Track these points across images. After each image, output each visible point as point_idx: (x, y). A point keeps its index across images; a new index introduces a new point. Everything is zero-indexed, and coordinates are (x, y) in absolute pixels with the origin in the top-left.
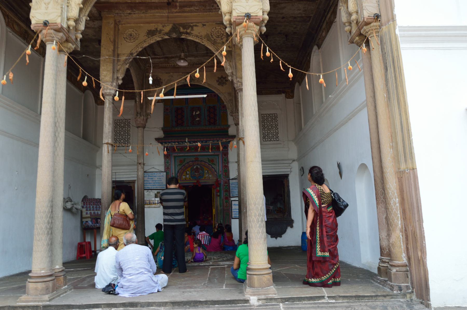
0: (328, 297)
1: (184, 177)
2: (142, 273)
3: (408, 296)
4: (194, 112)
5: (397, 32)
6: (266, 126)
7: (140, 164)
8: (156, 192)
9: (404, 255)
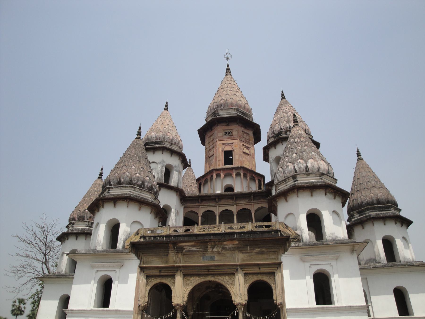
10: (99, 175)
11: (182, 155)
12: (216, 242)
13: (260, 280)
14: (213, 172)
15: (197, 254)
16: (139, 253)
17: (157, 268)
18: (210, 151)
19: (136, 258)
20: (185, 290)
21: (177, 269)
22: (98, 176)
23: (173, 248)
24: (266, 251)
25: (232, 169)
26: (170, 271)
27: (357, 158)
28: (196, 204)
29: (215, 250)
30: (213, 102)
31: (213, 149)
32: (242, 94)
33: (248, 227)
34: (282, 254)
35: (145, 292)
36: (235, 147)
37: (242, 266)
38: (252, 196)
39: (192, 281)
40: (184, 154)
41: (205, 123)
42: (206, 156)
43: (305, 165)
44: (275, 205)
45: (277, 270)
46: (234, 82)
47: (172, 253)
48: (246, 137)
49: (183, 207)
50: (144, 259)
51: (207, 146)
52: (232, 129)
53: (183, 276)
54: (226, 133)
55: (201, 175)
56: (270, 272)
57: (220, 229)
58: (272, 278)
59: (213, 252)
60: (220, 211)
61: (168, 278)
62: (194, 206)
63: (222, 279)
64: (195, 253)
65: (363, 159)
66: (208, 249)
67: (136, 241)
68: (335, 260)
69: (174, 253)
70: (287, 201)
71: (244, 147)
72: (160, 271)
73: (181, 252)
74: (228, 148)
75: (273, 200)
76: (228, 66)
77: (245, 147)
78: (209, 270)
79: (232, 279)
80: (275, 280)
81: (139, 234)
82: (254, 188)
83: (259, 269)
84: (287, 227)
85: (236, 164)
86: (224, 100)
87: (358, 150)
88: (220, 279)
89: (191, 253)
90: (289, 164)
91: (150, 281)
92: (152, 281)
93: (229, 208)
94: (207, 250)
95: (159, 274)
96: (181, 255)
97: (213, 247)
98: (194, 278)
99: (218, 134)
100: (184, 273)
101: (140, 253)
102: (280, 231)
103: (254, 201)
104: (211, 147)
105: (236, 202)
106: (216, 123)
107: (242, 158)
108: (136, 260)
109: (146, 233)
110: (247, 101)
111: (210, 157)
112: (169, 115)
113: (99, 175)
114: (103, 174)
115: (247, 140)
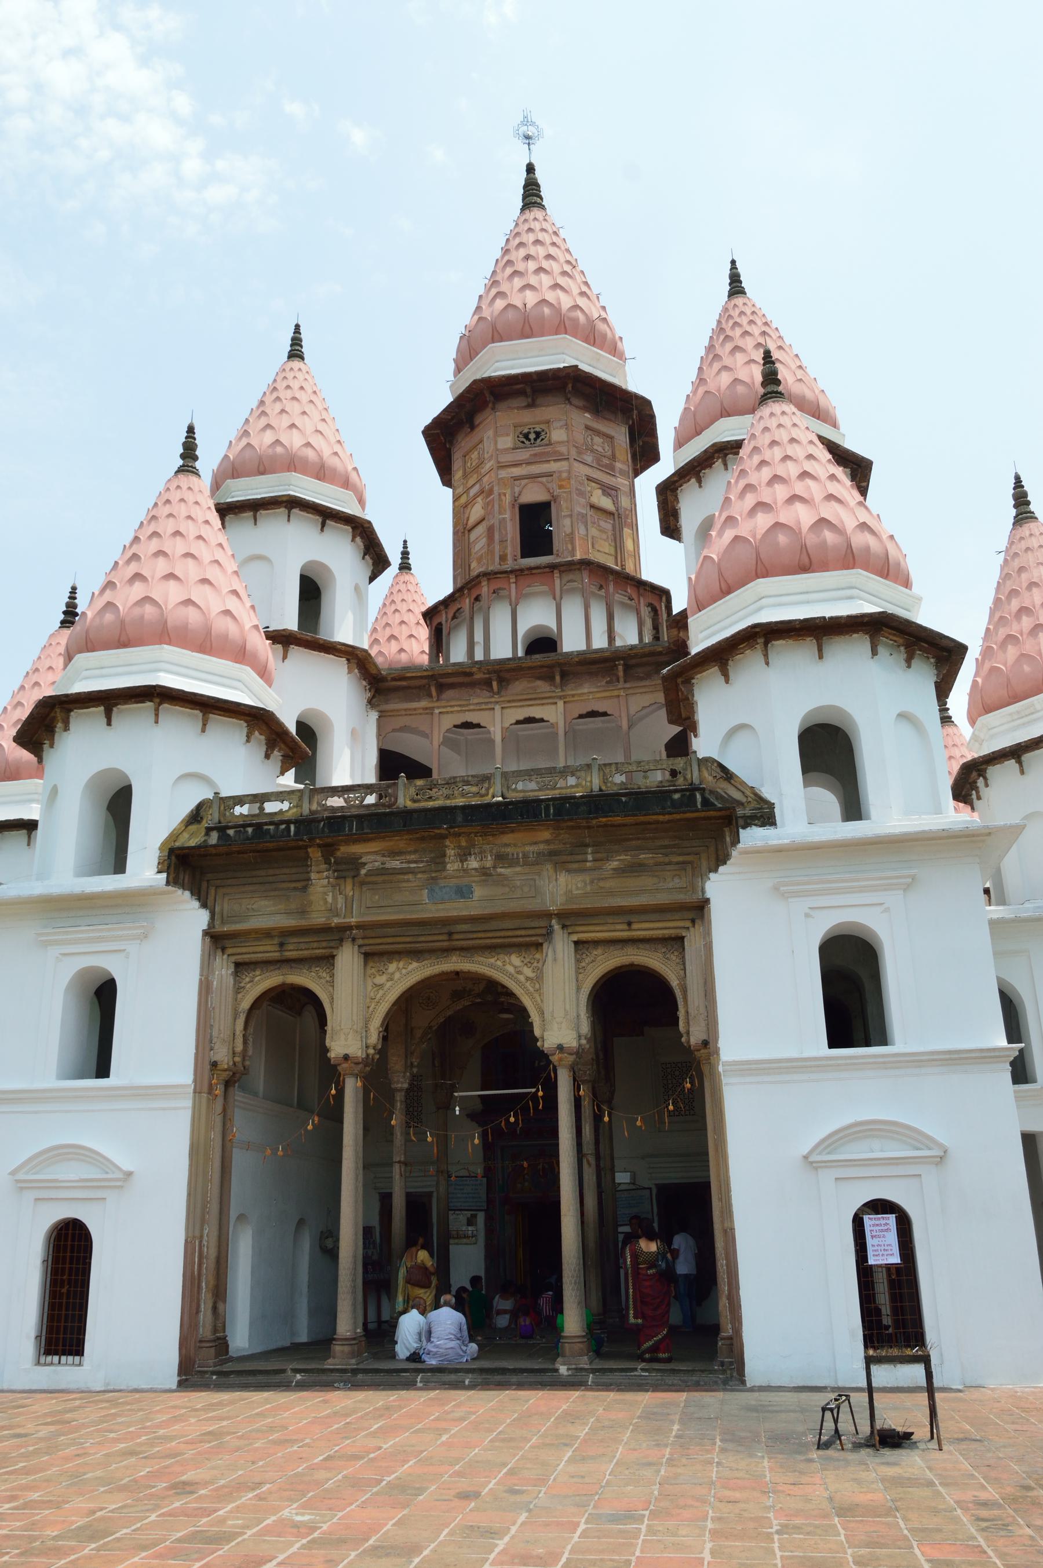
0: (641, 1369)
1: (519, 1186)
2: (450, 1340)
3: (729, 1372)
4: (537, 1062)
5: (721, 1069)
6: (670, 1086)
7: (442, 1172)
8: (469, 1214)
9: (730, 1326)
10: (64, 613)
11: (362, 526)
12: (473, 835)
13: (632, 965)
14: (480, 582)
15: (408, 881)
16: (204, 885)
17: (267, 934)
18: (469, 506)
19: (196, 904)
20: (371, 1009)
21: (338, 934)
22: (62, 617)
23: (326, 864)
24: (652, 861)
25: (547, 570)
26: (315, 945)
27: (1014, 512)
28: (419, 699)
29: (473, 863)
30: (476, 317)
31: (479, 499)
32: (586, 283)
33: (589, 779)
34: (710, 872)
35: (235, 1018)
36: (561, 487)
37: (569, 918)
38: (621, 668)
39: (393, 974)
40: (369, 522)
41: (449, 399)
42: (455, 525)
44: (688, 699)
45: (692, 929)
46: (555, 233)
47: (320, 881)
48: (600, 449)
49: (374, 716)
50: (225, 906)
51: (460, 490)
52: (548, 422)
53: (362, 960)
54: (526, 436)
55: (441, 597)
56: (667, 936)
57: (488, 789)
58: (674, 958)
59: (465, 871)
60: (507, 725)
61: (310, 967)
62: (415, 709)
63: (499, 963)
64: (402, 877)
65: (1037, 515)
66: (447, 860)
67: (193, 845)
68: (902, 892)
69: (329, 881)
71: (594, 484)
72: (281, 945)
73: (354, 877)
74: (533, 495)
75: (679, 680)
76: (530, 169)
77: (599, 486)
78: (450, 934)
79: (535, 964)
80: (684, 964)
81: (202, 818)
82: (629, 635)
83: (625, 927)
84: (727, 774)
85: (563, 551)
86: (515, 307)
87: (1018, 482)
88: (491, 966)
89: (386, 878)
91: (248, 979)
92: (257, 979)
93: (536, 712)
94: (444, 864)
95: (277, 954)
96: (354, 885)
97: (465, 855)
98: (401, 965)
99: (496, 443)
100: (363, 950)
101: (208, 887)
102: (704, 789)
103: (628, 685)
104: (473, 492)
105: (563, 690)
106: (488, 399)
107: (587, 530)
108: (194, 909)
109: (228, 814)
110: (604, 308)
111: (469, 531)
112: (307, 376)
113: (64, 613)
114: (77, 610)
115: (606, 461)
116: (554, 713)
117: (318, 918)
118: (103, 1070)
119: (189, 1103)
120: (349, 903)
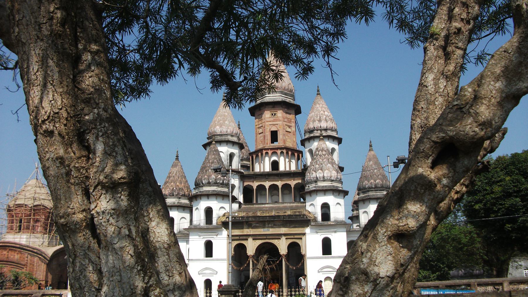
19: (225, 230)
37: (285, 235)
43: (322, 174)
54: (272, 114)
70: (311, 196)
74: (274, 129)
90: (313, 172)
104: (260, 125)
111: (259, 134)
116: (279, 184)
117: (245, 233)
118: (211, 256)
119: (226, 261)
120: (250, 231)
